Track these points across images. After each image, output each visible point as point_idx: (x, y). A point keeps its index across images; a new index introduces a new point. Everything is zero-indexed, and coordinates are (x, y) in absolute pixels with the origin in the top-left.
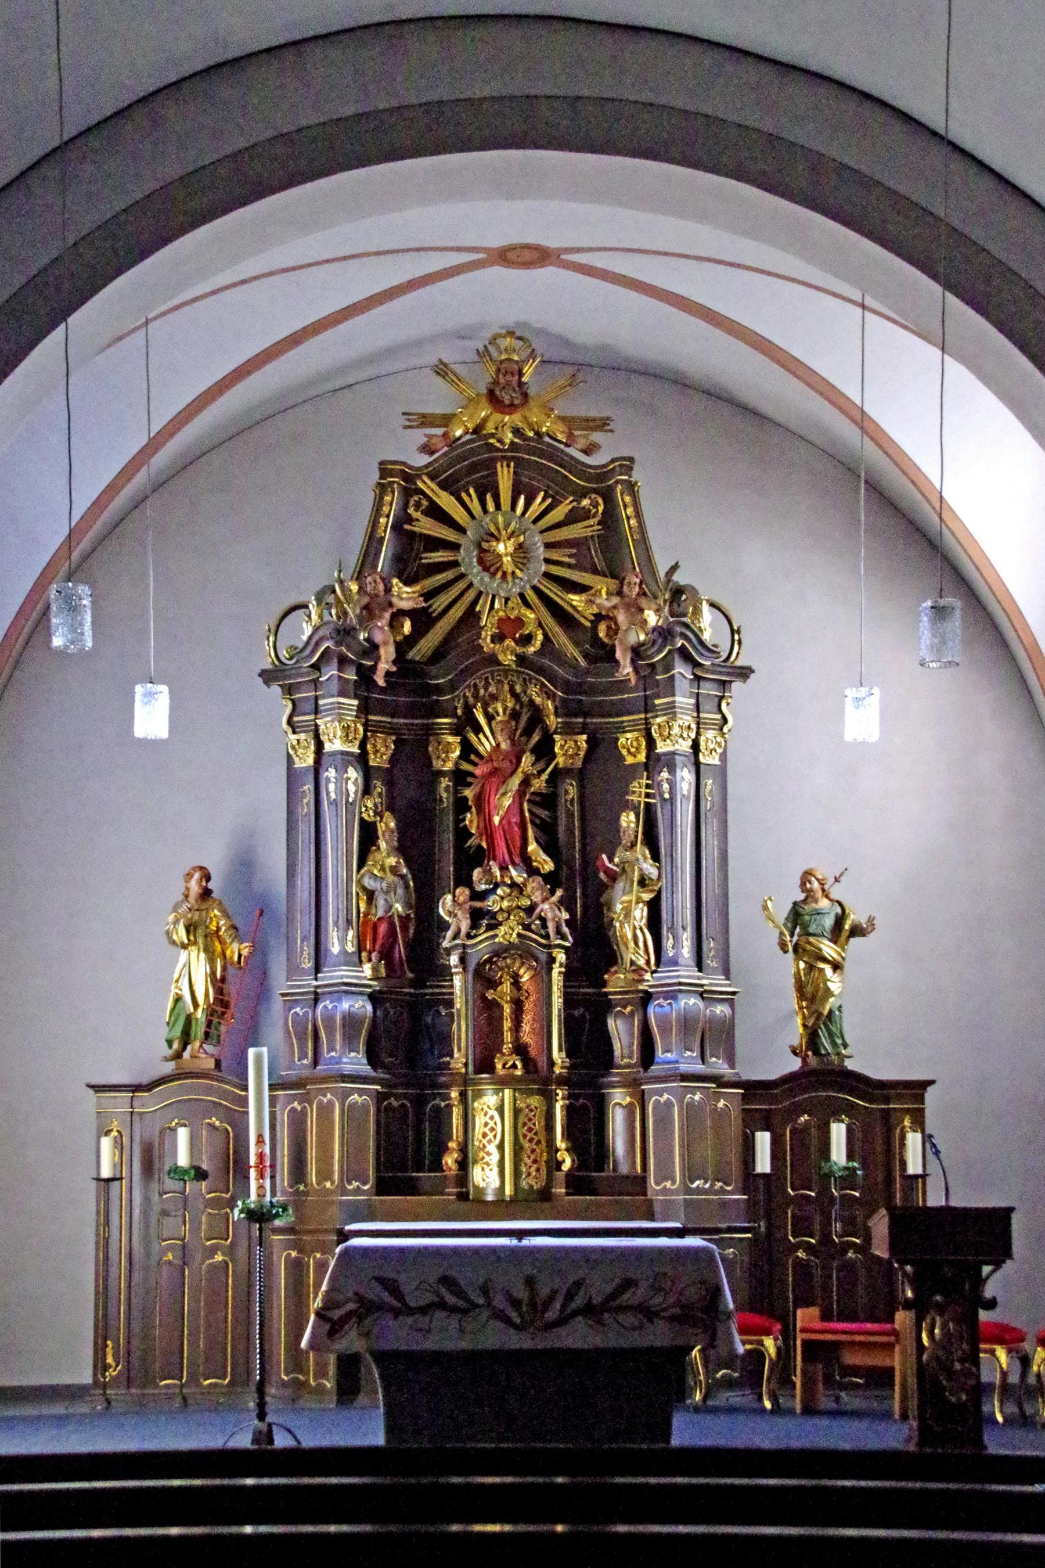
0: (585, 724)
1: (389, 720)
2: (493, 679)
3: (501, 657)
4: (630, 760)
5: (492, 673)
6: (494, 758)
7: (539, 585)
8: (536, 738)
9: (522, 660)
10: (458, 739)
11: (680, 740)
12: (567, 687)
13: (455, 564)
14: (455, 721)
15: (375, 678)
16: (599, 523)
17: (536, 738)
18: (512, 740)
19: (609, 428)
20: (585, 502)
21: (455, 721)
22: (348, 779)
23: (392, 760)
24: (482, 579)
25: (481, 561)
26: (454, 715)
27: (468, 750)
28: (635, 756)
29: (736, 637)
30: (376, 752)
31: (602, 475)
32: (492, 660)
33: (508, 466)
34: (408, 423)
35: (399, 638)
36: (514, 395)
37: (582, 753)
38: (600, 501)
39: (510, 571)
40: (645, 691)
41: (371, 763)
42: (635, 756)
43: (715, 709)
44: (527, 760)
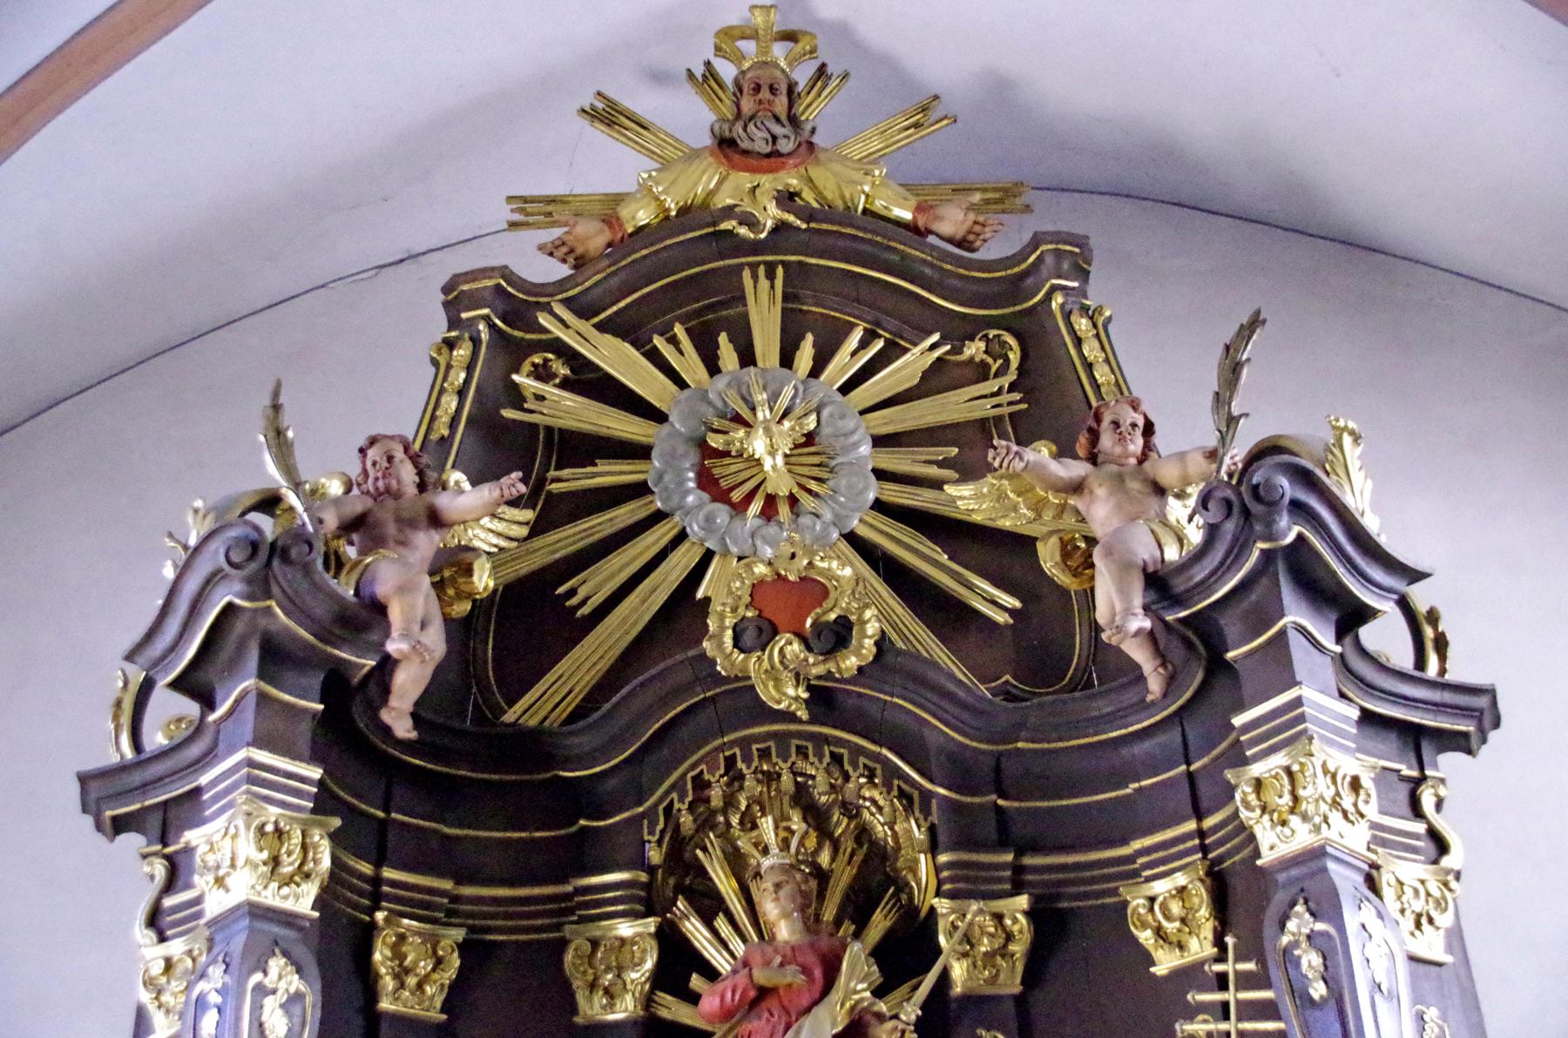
0: (1018, 869)
1: (447, 885)
2: (747, 759)
3: (767, 693)
4: (1165, 962)
5: (745, 743)
6: (756, 960)
7: (864, 532)
8: (880, 923)
9: (823, 699)
10: (651, 924)
11: (1335, 817)
12: (961, 772)
13: (640, 490)
14: (643, 877)
15: (386, 716)
16: (1013, 387)
17: (880, 923)
18: (811, 923)
19: (1019, 201)
20: (974, 349)
21: (643, 877)
22: (261, 991)
23: (456, 995)
24: (709, 519)
25: (707, 481)
26: (640, 862)
27: (678, 965)
28: (1181, 946)
29: (1429, 632)
30: (401, 974)
31: (1012, 285)
32: (744, 703)
33: (771, 276)
34: (518, 217)
35: (462, 608)
36: (778, 130)
37: (1018, 948)
38: (1011, 341)
39: (783, 492)
40: (1188, 764)
41: (385, 1005)
42: (1181, 946)
43: (1405, 808)
44: (857, 978)
